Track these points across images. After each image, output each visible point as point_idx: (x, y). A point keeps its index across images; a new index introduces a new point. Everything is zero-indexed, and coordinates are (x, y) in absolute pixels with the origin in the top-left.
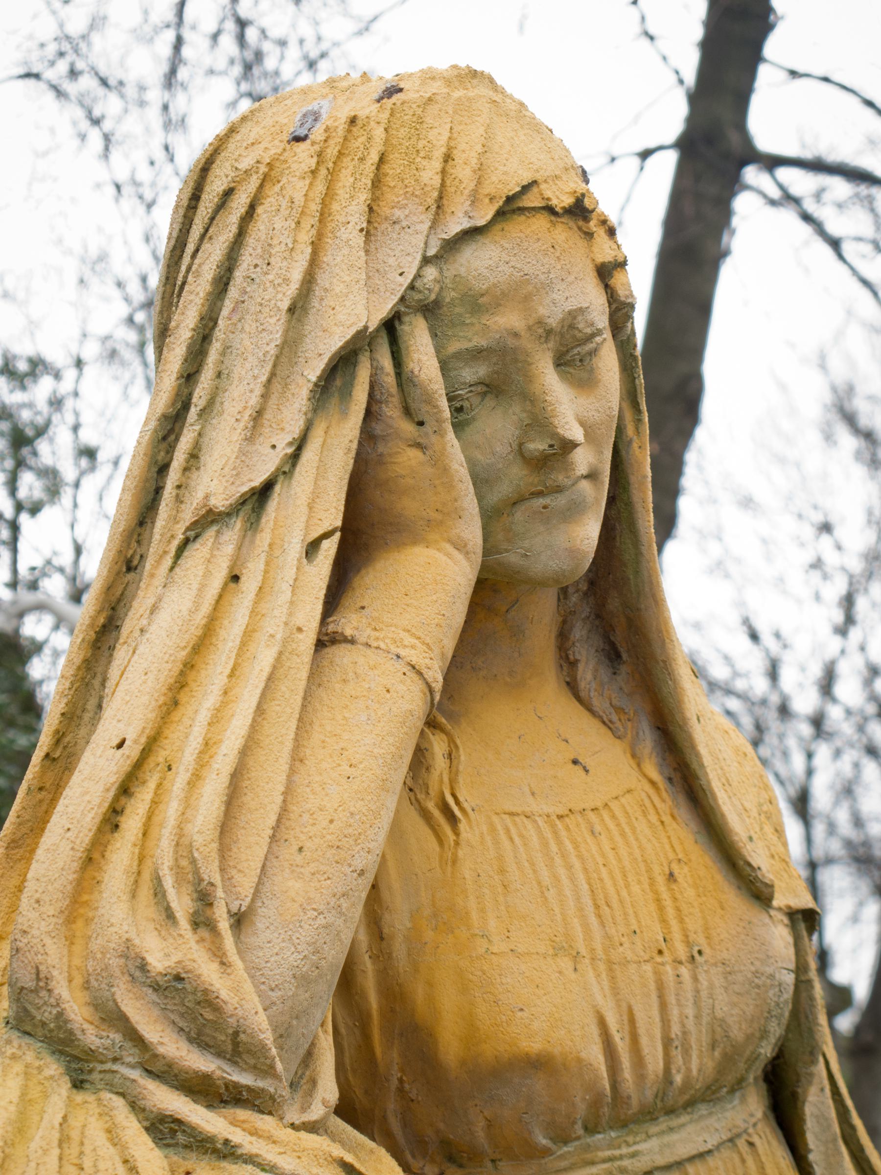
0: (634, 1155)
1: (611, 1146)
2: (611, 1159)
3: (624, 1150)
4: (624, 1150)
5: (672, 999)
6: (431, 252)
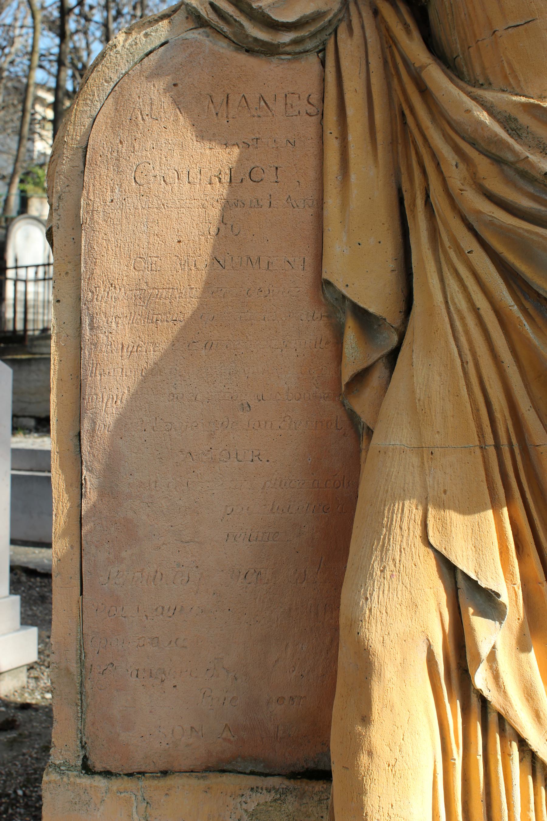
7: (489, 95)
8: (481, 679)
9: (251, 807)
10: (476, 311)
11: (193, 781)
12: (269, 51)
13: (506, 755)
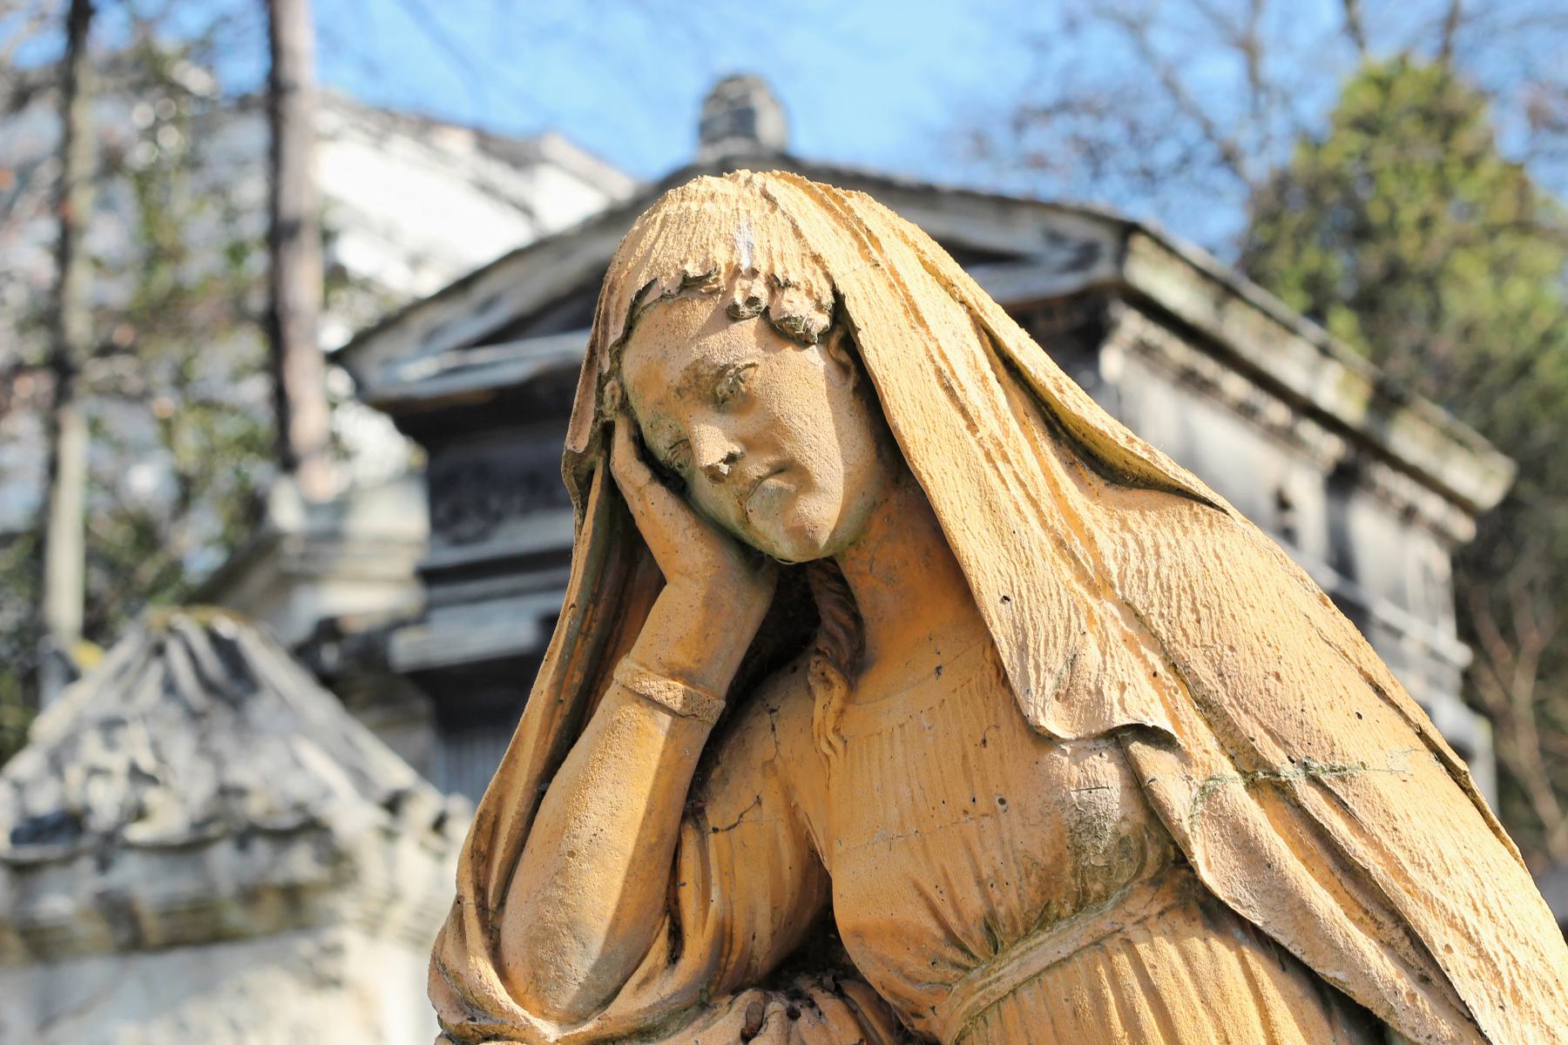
0: (999, 979)
1: (983, 976)
2: (983, 987)
3: (994, 976)
4: (994, 976)
5: (977, 849)
6: (606, 370)
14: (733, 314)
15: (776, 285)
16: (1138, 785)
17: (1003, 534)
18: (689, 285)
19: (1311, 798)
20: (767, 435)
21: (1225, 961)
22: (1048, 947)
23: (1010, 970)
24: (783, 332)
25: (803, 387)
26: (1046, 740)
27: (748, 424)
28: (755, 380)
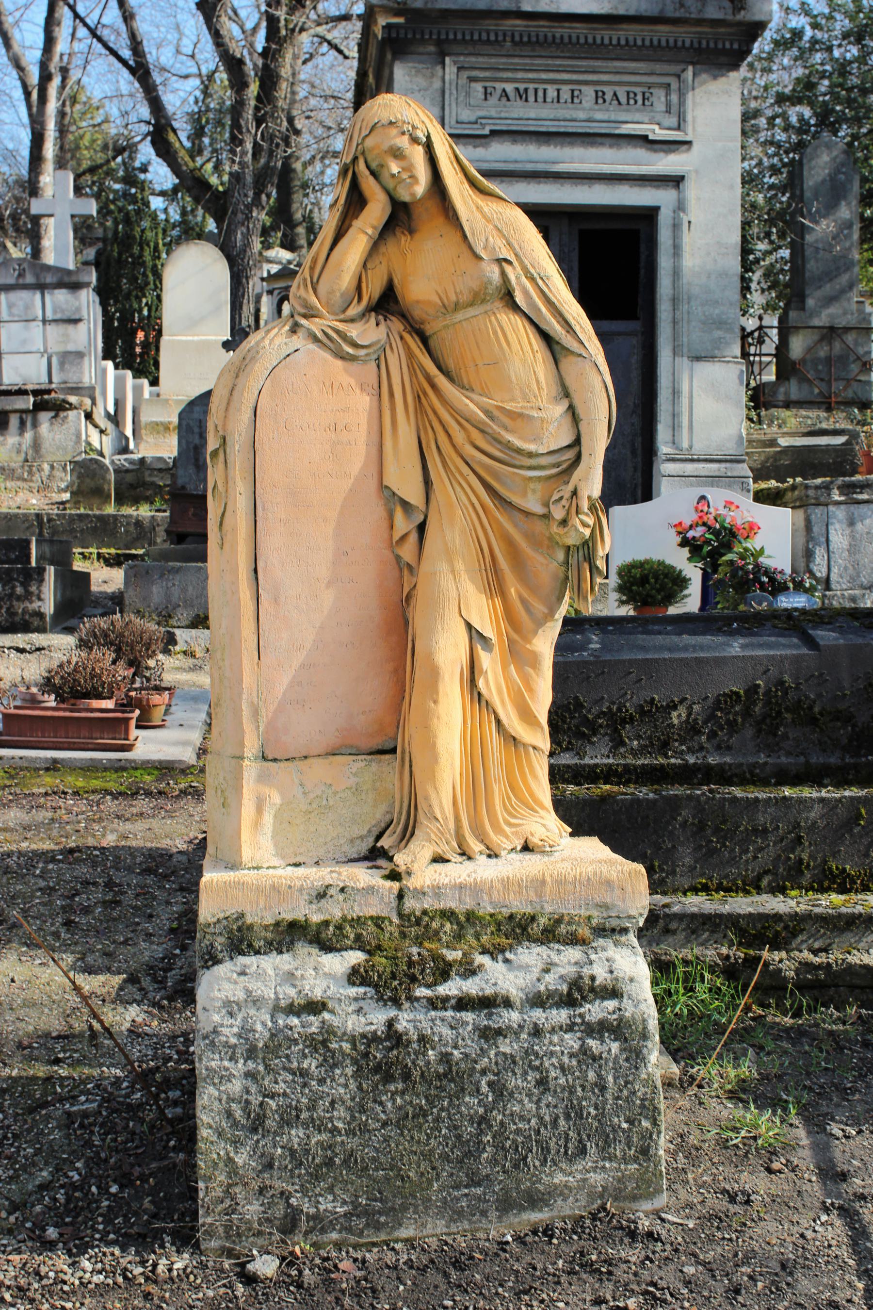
7: (474, 396)
8: (481, 683)
9: (354, 770)
10: (473, 505)
11: (320, 760)
12: (353, 358)
13: (490, 722)
14: (403, 133)
15: (413, 127)
16: (503, 274)
17: (465, 203)
18: (391, 123)
19: (540, 282)
20: (409, 168)
21: (518, 321)
22: (471, 312)
23: (459, 316)
24: (415, 140)
25: (418, 155)
26: (479, 258)
27: (404, 164)
28: (407, 152)
